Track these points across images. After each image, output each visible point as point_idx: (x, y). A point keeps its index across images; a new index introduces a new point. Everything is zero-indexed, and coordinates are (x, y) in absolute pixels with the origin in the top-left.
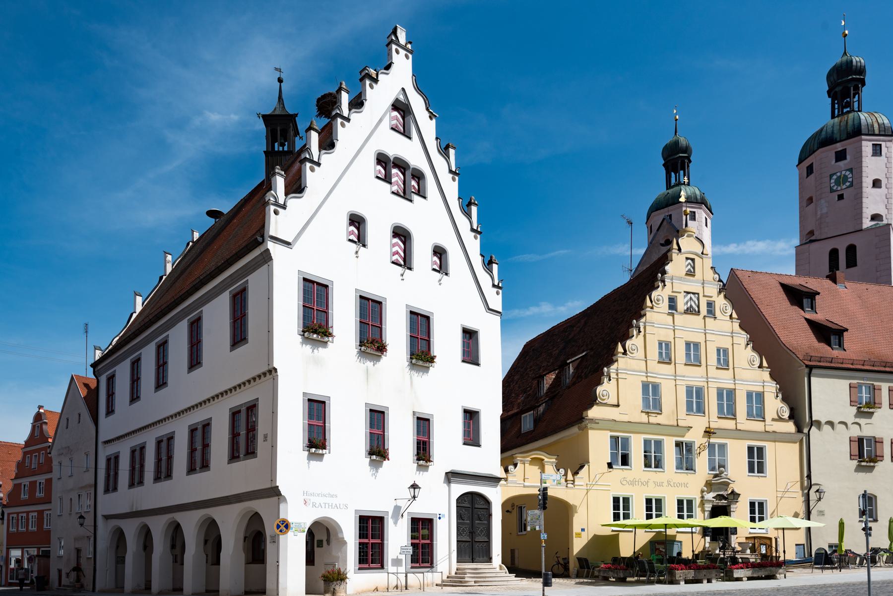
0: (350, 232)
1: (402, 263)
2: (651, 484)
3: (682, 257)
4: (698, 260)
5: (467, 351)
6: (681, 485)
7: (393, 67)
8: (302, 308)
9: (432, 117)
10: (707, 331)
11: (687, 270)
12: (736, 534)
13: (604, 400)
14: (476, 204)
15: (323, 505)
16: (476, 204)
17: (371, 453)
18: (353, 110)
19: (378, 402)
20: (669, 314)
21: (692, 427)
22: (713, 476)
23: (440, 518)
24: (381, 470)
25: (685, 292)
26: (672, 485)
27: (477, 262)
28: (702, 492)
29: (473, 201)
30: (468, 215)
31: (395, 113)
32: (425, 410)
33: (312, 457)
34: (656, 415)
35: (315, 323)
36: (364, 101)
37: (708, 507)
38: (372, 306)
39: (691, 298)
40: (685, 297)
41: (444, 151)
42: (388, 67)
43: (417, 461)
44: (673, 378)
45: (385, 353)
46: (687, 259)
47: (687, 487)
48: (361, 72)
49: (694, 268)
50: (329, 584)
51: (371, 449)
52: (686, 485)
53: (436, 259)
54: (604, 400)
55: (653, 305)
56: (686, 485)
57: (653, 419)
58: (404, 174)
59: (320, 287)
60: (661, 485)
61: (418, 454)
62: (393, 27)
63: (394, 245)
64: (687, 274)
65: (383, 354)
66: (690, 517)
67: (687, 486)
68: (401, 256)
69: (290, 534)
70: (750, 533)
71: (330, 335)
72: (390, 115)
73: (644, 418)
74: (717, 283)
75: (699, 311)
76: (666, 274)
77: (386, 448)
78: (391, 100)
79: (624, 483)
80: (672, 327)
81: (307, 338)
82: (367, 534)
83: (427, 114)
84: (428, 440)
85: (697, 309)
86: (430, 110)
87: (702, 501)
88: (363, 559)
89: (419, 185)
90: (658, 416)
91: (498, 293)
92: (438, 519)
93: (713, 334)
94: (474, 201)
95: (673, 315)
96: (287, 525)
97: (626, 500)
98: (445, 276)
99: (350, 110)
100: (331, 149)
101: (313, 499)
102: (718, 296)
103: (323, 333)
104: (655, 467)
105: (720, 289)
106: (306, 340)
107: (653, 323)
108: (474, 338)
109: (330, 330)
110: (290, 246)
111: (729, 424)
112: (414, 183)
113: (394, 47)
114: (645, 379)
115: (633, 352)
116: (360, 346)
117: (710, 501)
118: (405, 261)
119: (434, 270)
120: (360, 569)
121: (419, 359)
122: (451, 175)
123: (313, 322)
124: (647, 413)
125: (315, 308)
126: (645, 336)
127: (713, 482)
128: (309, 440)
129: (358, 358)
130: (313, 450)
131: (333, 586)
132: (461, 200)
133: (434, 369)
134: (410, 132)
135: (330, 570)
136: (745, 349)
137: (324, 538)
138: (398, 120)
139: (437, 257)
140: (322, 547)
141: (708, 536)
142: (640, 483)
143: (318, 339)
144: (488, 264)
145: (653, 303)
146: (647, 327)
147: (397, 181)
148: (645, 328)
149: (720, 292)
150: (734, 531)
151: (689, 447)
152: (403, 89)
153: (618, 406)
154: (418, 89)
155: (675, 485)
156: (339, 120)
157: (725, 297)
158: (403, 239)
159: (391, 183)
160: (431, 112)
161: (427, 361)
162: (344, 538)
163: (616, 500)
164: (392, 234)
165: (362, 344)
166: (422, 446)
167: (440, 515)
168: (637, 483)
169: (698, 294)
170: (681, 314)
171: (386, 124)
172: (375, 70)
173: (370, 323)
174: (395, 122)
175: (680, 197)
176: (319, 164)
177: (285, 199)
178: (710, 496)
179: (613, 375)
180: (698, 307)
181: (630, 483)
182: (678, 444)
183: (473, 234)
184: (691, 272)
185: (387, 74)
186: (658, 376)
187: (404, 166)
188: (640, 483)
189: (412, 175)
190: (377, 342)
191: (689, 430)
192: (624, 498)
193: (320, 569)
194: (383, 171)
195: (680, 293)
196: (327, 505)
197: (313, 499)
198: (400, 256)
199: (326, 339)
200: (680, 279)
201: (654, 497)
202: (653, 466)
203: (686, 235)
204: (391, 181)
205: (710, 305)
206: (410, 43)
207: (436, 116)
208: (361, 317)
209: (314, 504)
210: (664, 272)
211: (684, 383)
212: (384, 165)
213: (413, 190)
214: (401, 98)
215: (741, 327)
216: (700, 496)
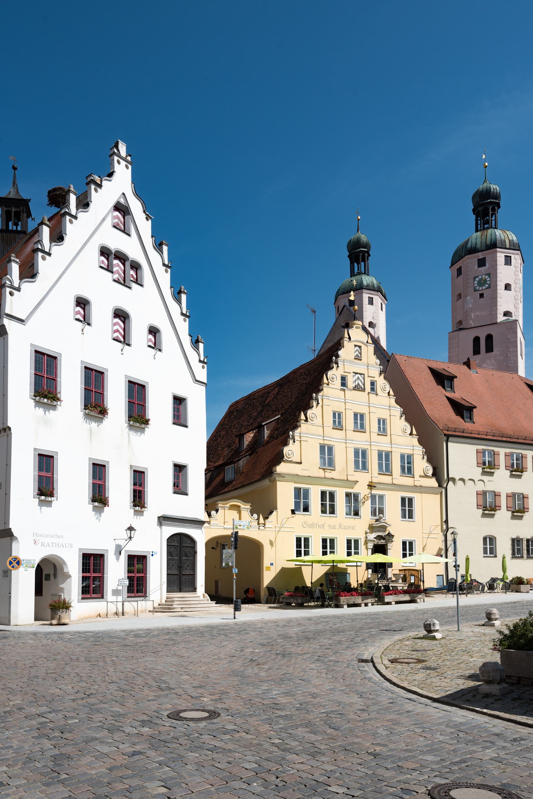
0: (76, 312)
1: (122, 340)
2: (326, 527)
3: (352, 344)
4: (363, 347)
5: (177, 415)
7: (115, 176)
8: (33, 376)
9: (148, 218)
10: (370, 405)
11: (355, 355)
12: (392, 567)
13: (290, 458)
14: (185, 293)
15: (51, 545)
16: (185, 293)
17: (94, 500)
18: (80, 210)
19: (100, 458)
20: (342, 390)
21: (358, 482)
22: (375, 520)
23: (152, 555)
24: (103, 515)
25: (354, 372)
26: (343, 528)
27: (186, 340)
28: (366, 533)
29: (182, 290)
30: (179, 301)
31: (117, 213)
32: (140, 465)
33: (42, 503)
34: (330, 471)
35: (45, 388)
36: (89, 202)
37: (371, 545)
38: (95, 375)
39: (358, 378)
40: (354, 376)
41: (158, 246)
42: (111, 175)
43: (134, 507)
44: (345, 441)
45: (106, 415)
46: (356, 346)
48: (87, 177)
49: (361, 354)
50: (55, 612)
51: (93, 496)
52: (353, 528)
53: (151, 337)
54: (290, 458)
55: (329, 382)
56: (353, 528)
57: (329, 475)
58: (124, 265)
59: (49, 359)
60: (334, 527)
61: (134, 501)
62: (116, 141)
63: (115, 324)
64: (355, 359)
65: (104, 416)
66: (357, 553)
67: (355, 528)
68: (121, 334)
69: (21, 569)
70: (403, 566)
71: (58, 399)
72: (112, 215)
73: (321, 474)
74: (378, 366)
75: (364, 389)
76: (339, 357)
77: (106, 496)
78: (113, 203)
79: (305, 526)
80: (344, 401)
81: (38, 401)
82: (89, 569)
83: (144, 216)
84: (143, 489)
86: (147, 213)
87: (366, 540)
88: (86, 591)
89: (137, 275)
90: (332, 472)
91: (203, 367)
92: (151, 556)
93: (375, 407)
94: (184, 290)
95: (344, 390)
96: (18, 561)
97: (307, 540)
98: (159, 352)
99: (77, 209)
100: (60, 242)
101: (42, 539)
102: (379, 377)
103: (52, 398)
104: (329, 513)
105: (380, 372)
106: (38, 404)
107: (329, 397)
108: (183, 404)
109: (58, 396)
110: (24, 323)
111: (386, 479)
112: (132, 272)
113: (116, 158)
114: (322, 442)
115: (313, 419)
116: (84, 409)
117: (372, 541)
118: (124, 337)
119: (149, 346)
120: (83, 598)
121: (136, 422)
122: (164, 268)
123: (44, 388)
124: (324, 469)
125: (45, 376)
126: (322, 406)
127: (374, 525)
128: (39, 489)
129: (84, 419)
130: (43, 498)
131: (59, 613)
132: (172, 289)
133: (149, 430)
134: (129, 230)
135: (56, 600)
136: (400, 419)
137: (52, 573)
138: (119, 219)
139: (152, 335)
140: (49, 580)
141: (370, 569)
142: (318, 526)
143: (48, 403)
144: (196, 343)
145: (329, 380)
146: (324, 400)
147: (118, 271)
148: (322, 400)
149: (380, 374)
150: (390, 565)
151: (356, 496)
152: (123, 194)
153: (301, 463)
154: (138, 194)
155: (345, 528)
156: (68, 218)
157: (385, 378)
158: (123, 319)
159: (112, 272)
160: (147, 214)
161: (143, 423)
162: (69, 572)
163: (298, 540)
164: (113, 315)
165: (86, 407)
166: (137, 494)
167: (152, 552)
168: (315, 526)
169: (364, 374)
170: (350, 390)
171: (109, 222)
172: (99, 177)
173: (94, 390)
174: (116, 221)
175: (351, 296)
176: (49, 254)
177: (20, 283)
178: (372, 536)
179: (297, 438)
180: (364, 385)
182: (348, 495)
183: (183, 317)
184: (359, 357)
185: (110, 181)
186: (332, 440)
187: (124, 258)
188: (318, 526)
189: (131, 266)
190: (99, 406)
191: (356, 484)
193: (48, 599)
194: (106, 262)
195: (350, 373)
196: (54, 545)
197: (42, 539)
198: (121, 334)
199: (55, 403)
200: (350, 362)
201: (328, 537)
202: (328, 512)
203: (355, 326)
204: (113, 269)
206: (130, 156)
207: (151, 218)
208: (85, 385)
209: (43, 543)
210: (337, 356)
212: (107, 256)
213: (132, 279)
214: (122, 201)
215: (396, 402)
216: (365, 536)
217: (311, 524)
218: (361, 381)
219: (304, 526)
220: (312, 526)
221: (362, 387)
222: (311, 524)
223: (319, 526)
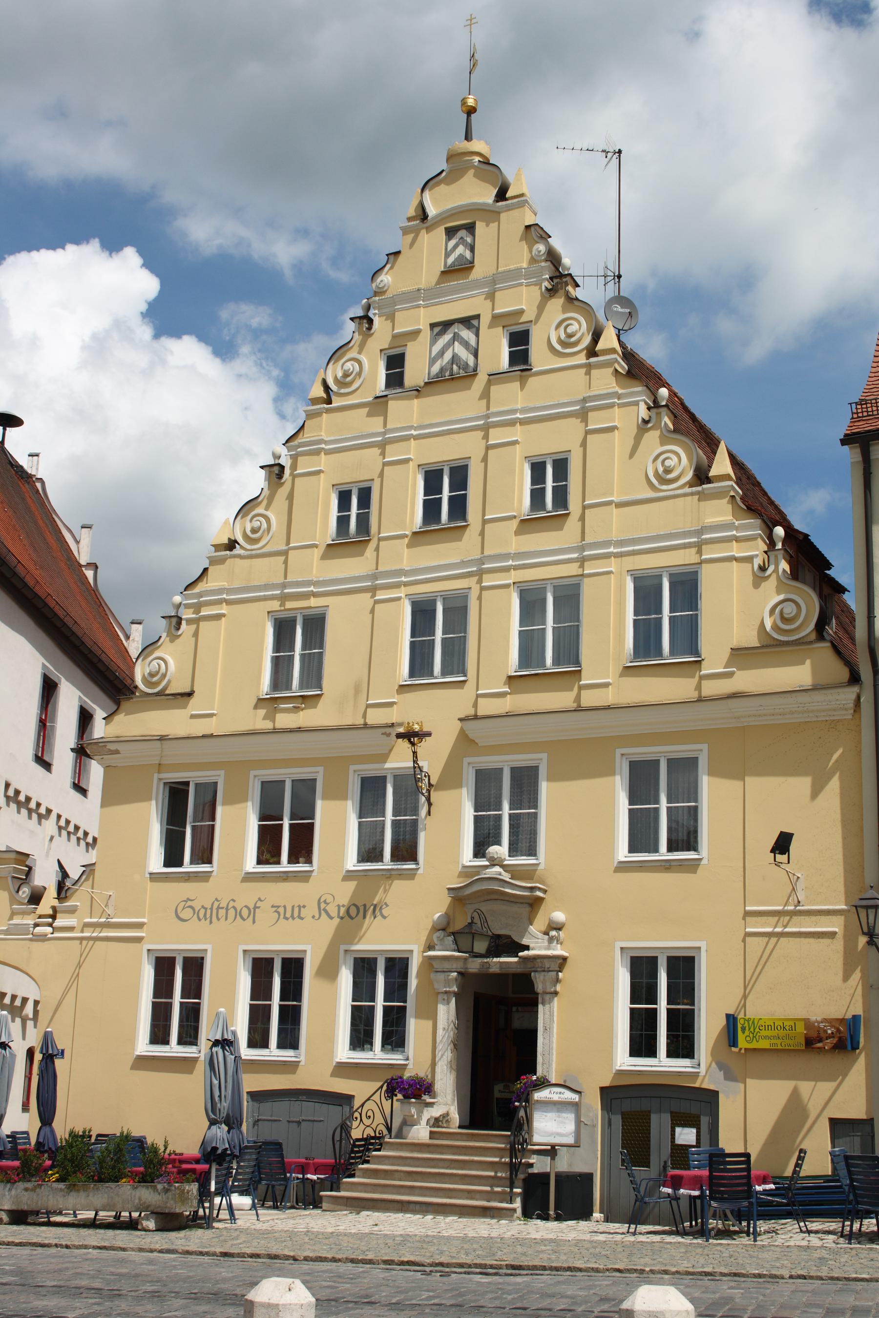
2: (265, 915)
11: (451, 260)
47: (384, 917)
49: (472, 249)
60: (296, 913)
75: (476, 365)
79: (186, 914)
85: (471, 361)
142: (232, 912)
168: (222, 912)
180: (476, 355)
181: (202, 911)
188: (232, 912)
211: (401, 593)
219: (181, 915)
223: (239, 914)
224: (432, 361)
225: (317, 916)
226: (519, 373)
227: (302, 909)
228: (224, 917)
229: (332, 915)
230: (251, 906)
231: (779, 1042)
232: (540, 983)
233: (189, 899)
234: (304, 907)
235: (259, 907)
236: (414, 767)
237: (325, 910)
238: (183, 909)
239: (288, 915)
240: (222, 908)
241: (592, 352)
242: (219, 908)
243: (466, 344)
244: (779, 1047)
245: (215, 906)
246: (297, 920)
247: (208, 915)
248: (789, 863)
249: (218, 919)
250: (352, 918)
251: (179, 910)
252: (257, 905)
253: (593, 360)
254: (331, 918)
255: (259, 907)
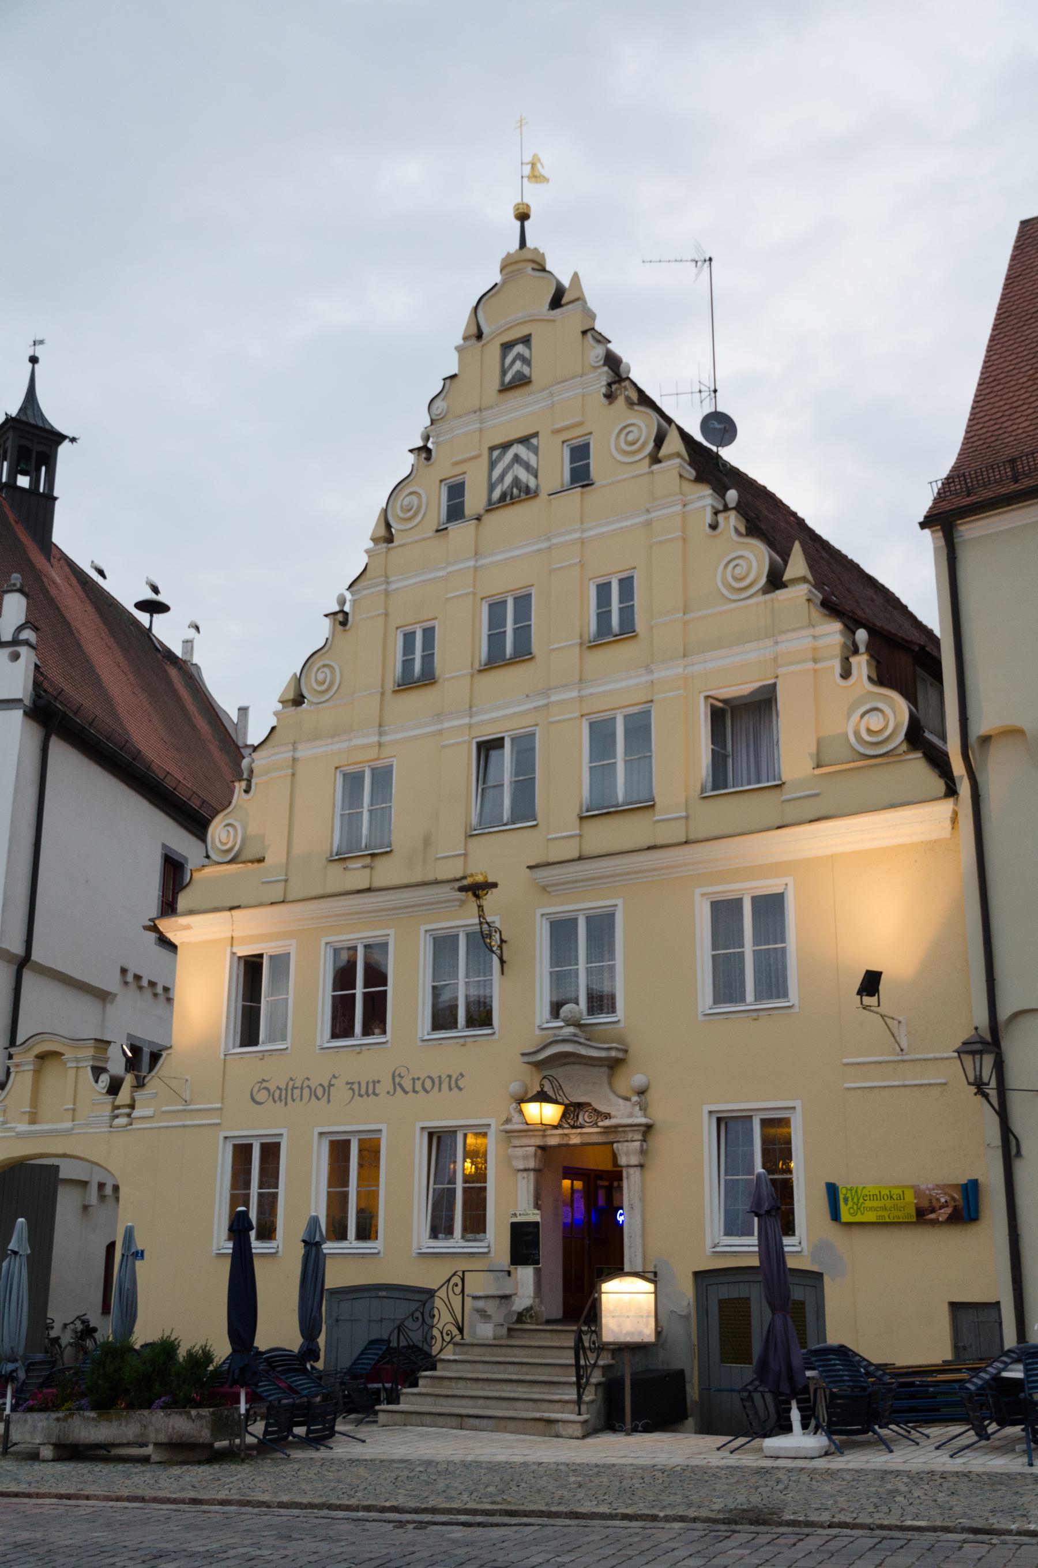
2: (340, 1093)
6: (437, 1082)
11: (508, 377)
26: (409, 1088)
39: (517, 458)
47: (460, 1089)
52: (455, 1083)
56: (455, 1083)
67: (461, 1084)
79: (262, 1096)
85: (532, 483)
142: (306, 1092)
155: (418, 1087)
168: (297, 1092)
181: (278, 1092)
188: (306, 1092)
192: (264, 1146)
205: (580, 453)
217: (283, 1087)
218: (527, 467)
219: (258, 1098)
220: (285, 1095)
221: (527, 490)
222: (283, 1087)
224: (492, 487)
225: (392, 1092)
226: (579, 489)
227: (377, 1085)
228: (299, 1098)
229: (407, 1089)
230: (326, 1085)
231: (886, 1214)
232: (628, 1153)
233: (264, 1080)
234: (379, 1082)
235: (333, 1085)
236: (481, 923)
237: (400, 1085)
238: (259, 1091)
239: (363, 1092)
240: (297, 1088)
241: (655, 459)
242: (293, 1088)
243: (527, 467)
244: (887, 1220)
245: (290, 1087)
246: (372, 1096)
247: (283, 1096)
248: (879, 1005)
249: (293, 1100)
250: (427, 1092)
251: (254, 1094)
252: (332, 1083)
253: (655, 467)
254: (406, 1093)
255: (333, 1085)
